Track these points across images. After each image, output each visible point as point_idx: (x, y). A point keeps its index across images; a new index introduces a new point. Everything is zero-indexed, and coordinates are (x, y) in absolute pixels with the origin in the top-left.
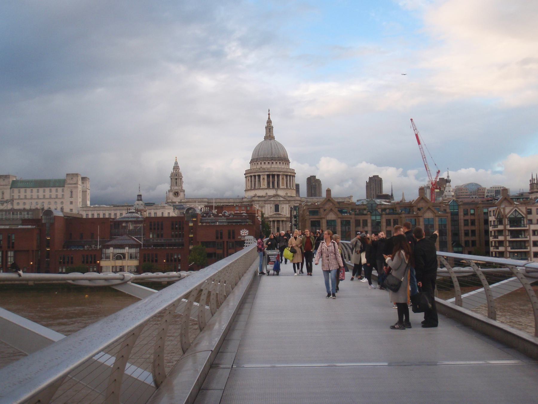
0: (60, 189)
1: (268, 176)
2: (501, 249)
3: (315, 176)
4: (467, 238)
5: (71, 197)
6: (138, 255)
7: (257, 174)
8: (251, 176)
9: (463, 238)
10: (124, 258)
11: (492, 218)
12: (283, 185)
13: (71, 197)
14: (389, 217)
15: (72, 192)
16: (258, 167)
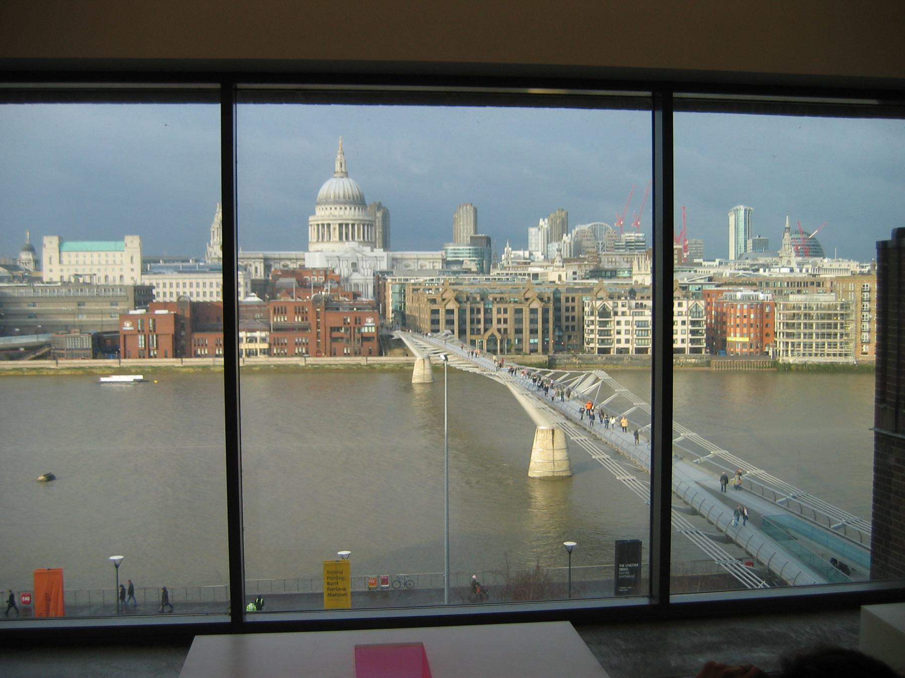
0: (118, 254)
1: (341, 225)
2: (592, 336)
3: (380, 203)
4: (567, 324)
5: (132, 262)
6: (268, 339)
7: (326, 222)
8: (318, 225)
9: (564, 323)
10: (256, 341)
11: (586, 309)
12: (359, 237)
13: (132, 262)
14: (499, 306)
15: (132, 258)
16: (328, 212)
